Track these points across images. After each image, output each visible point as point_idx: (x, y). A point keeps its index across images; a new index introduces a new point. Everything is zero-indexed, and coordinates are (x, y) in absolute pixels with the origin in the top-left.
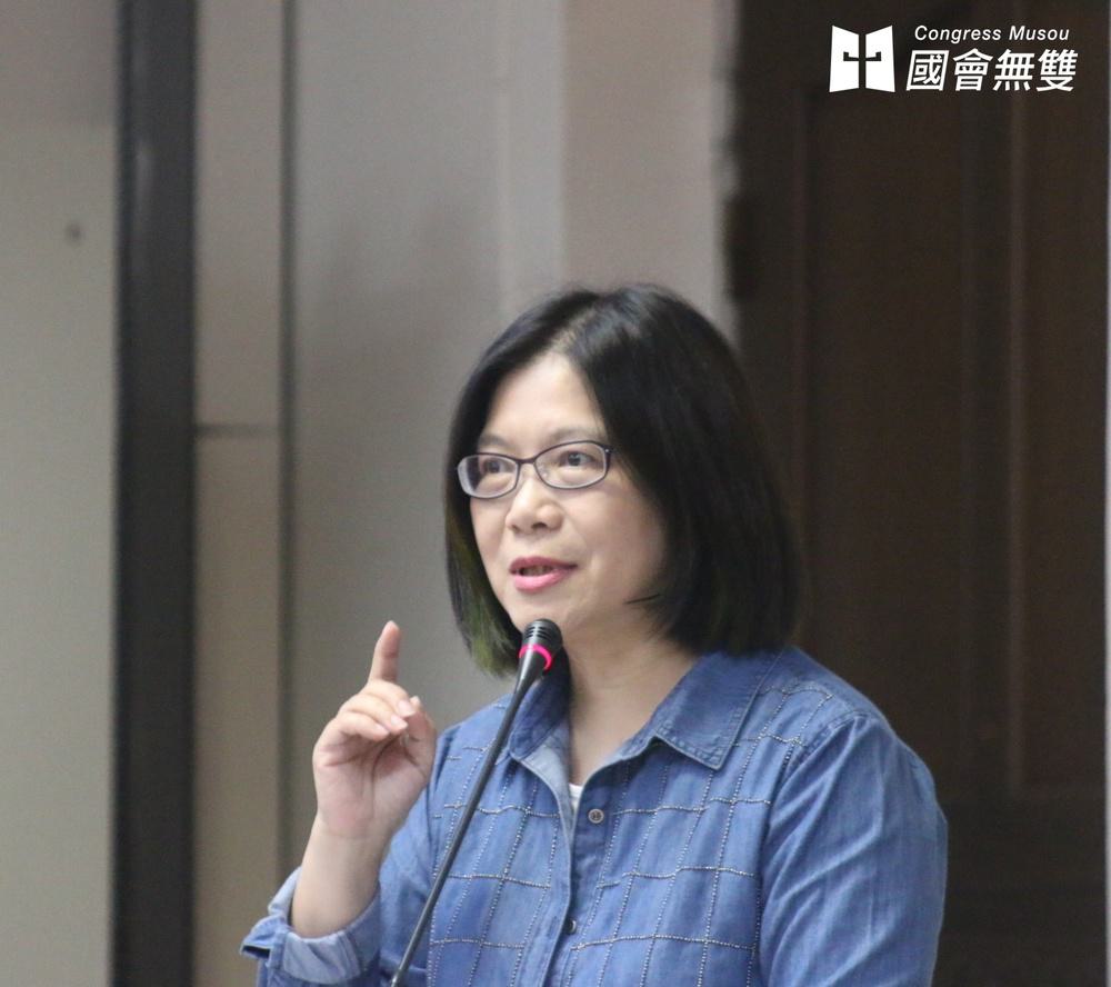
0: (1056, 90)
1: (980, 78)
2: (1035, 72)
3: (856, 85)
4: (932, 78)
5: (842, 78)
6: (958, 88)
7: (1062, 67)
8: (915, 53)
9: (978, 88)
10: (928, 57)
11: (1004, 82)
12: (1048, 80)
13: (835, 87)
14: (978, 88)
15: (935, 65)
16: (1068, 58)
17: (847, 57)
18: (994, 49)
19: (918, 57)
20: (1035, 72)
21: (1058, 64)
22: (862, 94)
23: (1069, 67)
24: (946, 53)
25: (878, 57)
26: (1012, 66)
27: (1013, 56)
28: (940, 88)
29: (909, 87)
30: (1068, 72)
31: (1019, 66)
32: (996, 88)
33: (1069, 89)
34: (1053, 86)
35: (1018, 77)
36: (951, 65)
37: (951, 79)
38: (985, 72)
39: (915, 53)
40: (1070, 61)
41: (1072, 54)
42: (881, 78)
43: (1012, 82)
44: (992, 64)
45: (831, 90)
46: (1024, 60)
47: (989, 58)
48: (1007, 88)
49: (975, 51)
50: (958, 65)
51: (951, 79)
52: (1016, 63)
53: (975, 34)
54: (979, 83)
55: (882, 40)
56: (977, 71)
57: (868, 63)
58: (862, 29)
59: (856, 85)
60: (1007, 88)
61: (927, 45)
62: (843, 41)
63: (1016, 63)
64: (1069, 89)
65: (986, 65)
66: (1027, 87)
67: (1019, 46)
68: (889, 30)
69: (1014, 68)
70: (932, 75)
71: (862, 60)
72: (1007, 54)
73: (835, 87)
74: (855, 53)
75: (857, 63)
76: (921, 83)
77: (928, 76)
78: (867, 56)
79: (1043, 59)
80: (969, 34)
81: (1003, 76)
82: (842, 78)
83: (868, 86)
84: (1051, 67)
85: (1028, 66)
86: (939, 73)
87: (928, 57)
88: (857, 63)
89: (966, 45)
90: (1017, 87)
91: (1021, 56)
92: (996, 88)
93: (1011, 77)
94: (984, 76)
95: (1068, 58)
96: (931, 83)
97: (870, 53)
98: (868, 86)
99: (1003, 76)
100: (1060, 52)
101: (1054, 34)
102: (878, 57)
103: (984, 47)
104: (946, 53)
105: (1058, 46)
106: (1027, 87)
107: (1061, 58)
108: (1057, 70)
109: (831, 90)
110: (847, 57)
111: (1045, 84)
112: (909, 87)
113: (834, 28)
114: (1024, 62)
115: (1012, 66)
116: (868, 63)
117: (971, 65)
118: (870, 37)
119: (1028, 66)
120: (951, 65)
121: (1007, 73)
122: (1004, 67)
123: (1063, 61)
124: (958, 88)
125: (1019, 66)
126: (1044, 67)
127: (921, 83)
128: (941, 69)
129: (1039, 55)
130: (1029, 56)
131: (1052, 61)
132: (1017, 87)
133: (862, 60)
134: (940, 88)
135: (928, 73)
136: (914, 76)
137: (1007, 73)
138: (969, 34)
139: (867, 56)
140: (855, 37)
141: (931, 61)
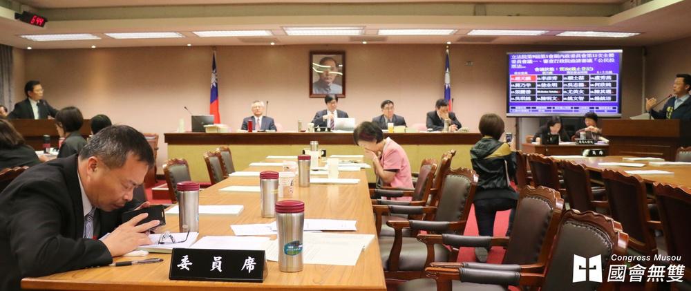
0: (675, 282)
1: (641, 277)
2: (666, 274)
3: (585, 280)
4: (619, 276)
5: (578, 276)
6: (631, 281)
7: (678, 272)
8: (611, 266)
9: (640, 281)
10: (617, 267)
11: (652, 278)
12: (672, 277)
13: (575, 280)
14: (640, 281)
15: (620, 271)
16: (681, 268)
17: (580, 268)
18: (647, 265)
19: (613, 267)
20: (666, 274)
21: (676, 271)
22: (588, 284)
23: (681, 272)
24: (625, 266)
25: (595, 268)
26: (655, 272)
27: (656, 267)
28: (623, 281)
29: (609, 280)
30: (681, 274)
31: (659, 272)
32: (648, 281)
33: (681, 281)
34: (674, 280)
35: (658, 276)
36: (628, 271)
37: (628, 277)
38: (643, 274)
39: (611, 266)
40: (681, 269)
41: (683, 266)
42: (596, 276)
43: (655, 278)
44: (646, 271)
45: (574, 281)
46: (661, 270)
47: (645, 268)
48: (653, 280)
49: (639, 265)
50: (631, 271)
51: (628, 277)
52: (657, 270)
53: (639, 258)
54: (641, 279)
55: (596, 261)
56: (640, 274)
57: (590, 270)
58: (587, 257)
59: (585, 280)
60: (653, 280)
61: (617, 262)
62: (579, 261)
63: (657, 270)
64: (681, 281)
65: (643, 271)
66: (662, 280)
67: (658, 263)
68: (600, 256)
69: (656, 273)
70: (619, 275)
71: (588, 269)
72: (653, 266)
73: (575, 280)
74: (584, 266)
75: (585, 270)
76: (614, 279)
77: (617, 275)
78: (590, 267)
79: (669, 268)
80: (636, 258)
81: (651, 276)
82: (578, 276)
83: (590, 280)
84: (673, 272)
85: (662, 271)
86: (622, 275)
87: (617, 267)
88: (585, 270)
89: (635, 262)
90: (658, 280)
91: (659, 267)
92: (648, 281)
93: (655, 276)
94: (643, 276)
95: (681, 268)
96: (618, 279)
97: (591, 266)
98: (590, 280)
99: (651, 276)
100: (677, 265)
101: (674, 258)
102: (595, 268)
103: (642, 263)
104: (625, 266)
105: (676, 263)
106: (662, 280)
107: (678, 268)
108: (676, 273)
109: (574, 281)
110: (580, 268)
111: (670, 279)
112: (609, 280)
113: (575, 256)
114: (661, 270)
115: (655, 272)
116: (590, 270)
117: (637, 271)
118: (590, 259)
119: (662, 271)
120: (628, 271)
121: (653, 274)
122: (652, 272)
123: (678, 269)
124: (631, 281)
125: (659, 272)
126: (670, 272)
127: (614, 279)
128: (622, 275)
129: (667, 266)
130: (663, 267)
131: (673, 270)
132: (658, 280)
133: (588, 269)
134: (623, 281)
135: (617, 275)
136: (611, 276)
137: (653, 274)
138: (636, 258)
139: (590, 267)
140: (584, 259)
141: (619, 269)
